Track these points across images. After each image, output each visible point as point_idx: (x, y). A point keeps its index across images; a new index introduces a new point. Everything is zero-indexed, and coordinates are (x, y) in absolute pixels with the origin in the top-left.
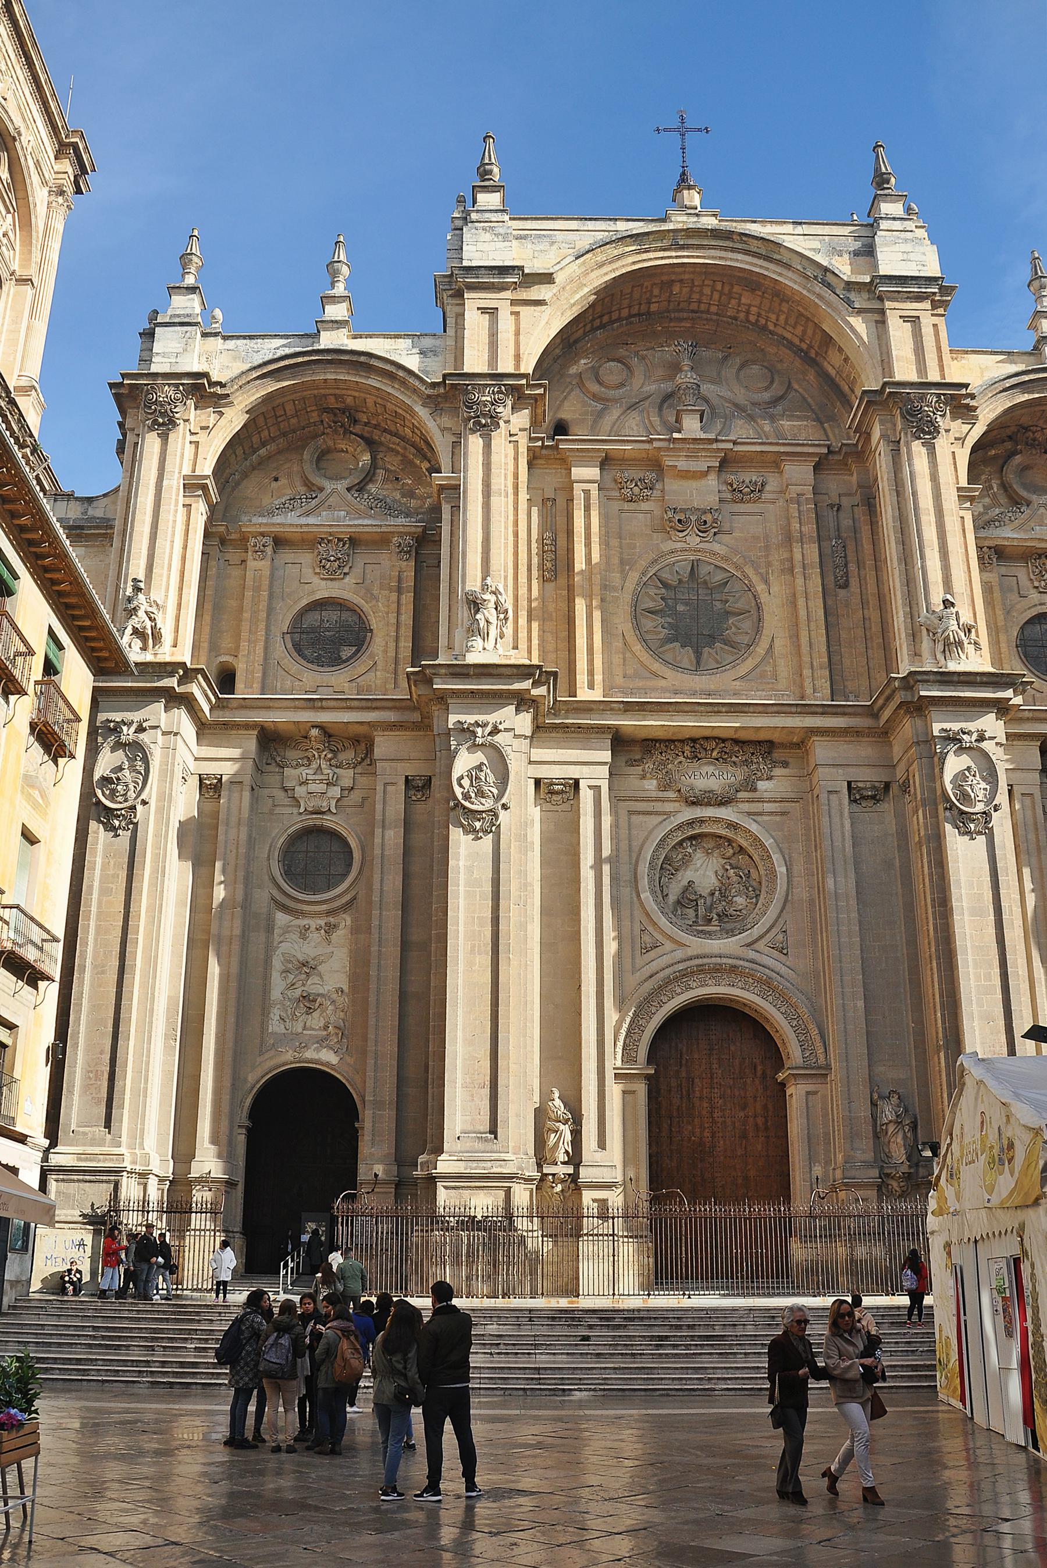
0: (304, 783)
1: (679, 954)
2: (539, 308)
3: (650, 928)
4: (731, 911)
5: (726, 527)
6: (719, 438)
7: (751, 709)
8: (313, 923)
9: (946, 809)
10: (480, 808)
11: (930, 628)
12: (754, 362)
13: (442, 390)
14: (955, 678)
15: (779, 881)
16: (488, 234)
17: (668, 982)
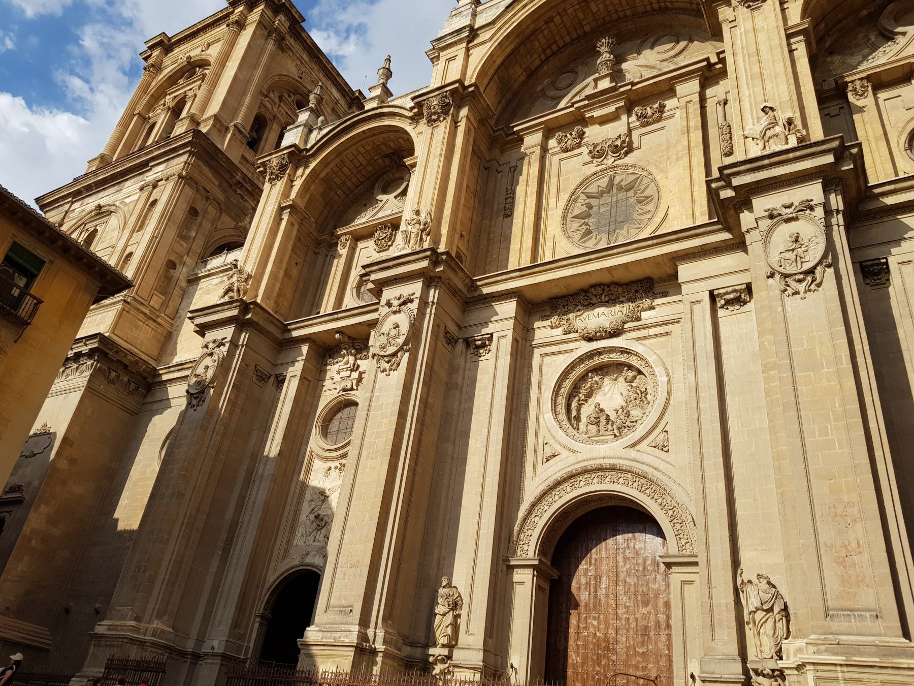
0: (338, 373)
1: (572, 459)
2: (485, 45)
3: (552, 442)
4: (628, 423)
5: (635, 145)
6: (619, 85)
7: (615, 251)
8: (333, 464)
9: (768, 277)
10: (387, 353)
11: (754, 136)
12: (664, 36)
13: (416, 110)
14: (766, 162)
15: (660, 389)
16: (458, 18)
17: (558, 484)
